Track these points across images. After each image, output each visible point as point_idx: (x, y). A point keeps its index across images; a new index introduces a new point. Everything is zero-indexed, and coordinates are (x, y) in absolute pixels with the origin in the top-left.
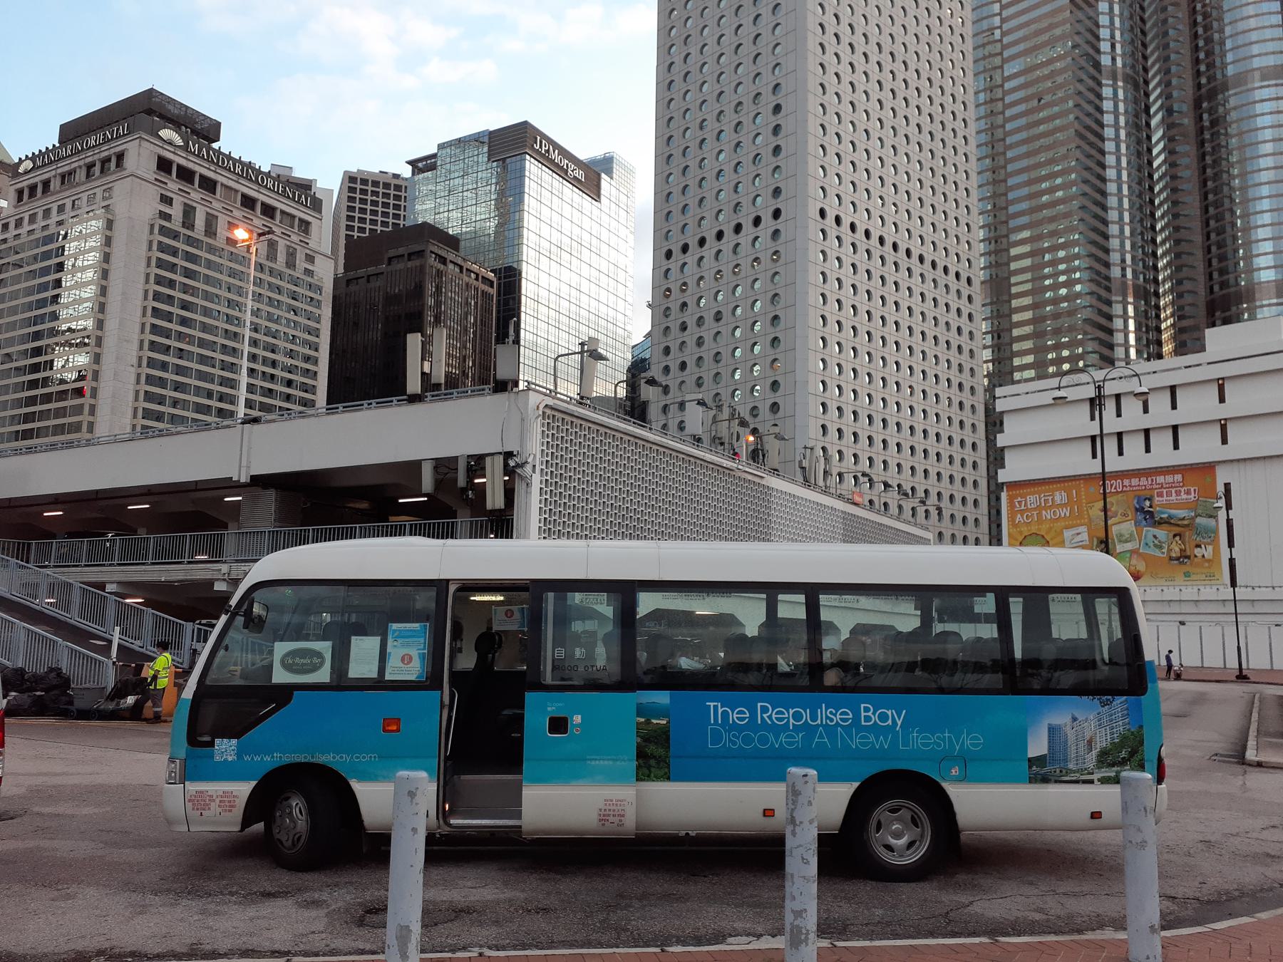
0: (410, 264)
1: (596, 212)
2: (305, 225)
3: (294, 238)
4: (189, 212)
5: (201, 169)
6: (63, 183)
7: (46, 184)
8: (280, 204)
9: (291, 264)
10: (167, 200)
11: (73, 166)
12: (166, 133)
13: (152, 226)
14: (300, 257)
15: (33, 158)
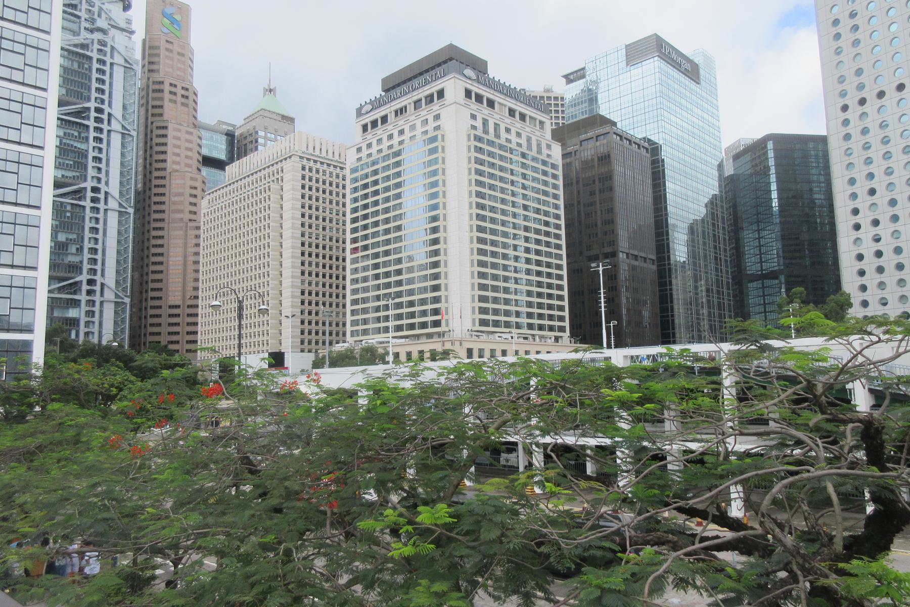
0: (598, 143)
1: (698, 90)
2: (541, 123)
3: (538, 133)
4: (485, 123)
5: (487, 93)
6: (396, 115)
7: (384, 119)
8: (529, 112)
9: (539, 152)
10: (473, 117)
11: (403, 104)
12: (469, 72)
13: (469, 136)
14: (544, 146)
15: (371, 102)
